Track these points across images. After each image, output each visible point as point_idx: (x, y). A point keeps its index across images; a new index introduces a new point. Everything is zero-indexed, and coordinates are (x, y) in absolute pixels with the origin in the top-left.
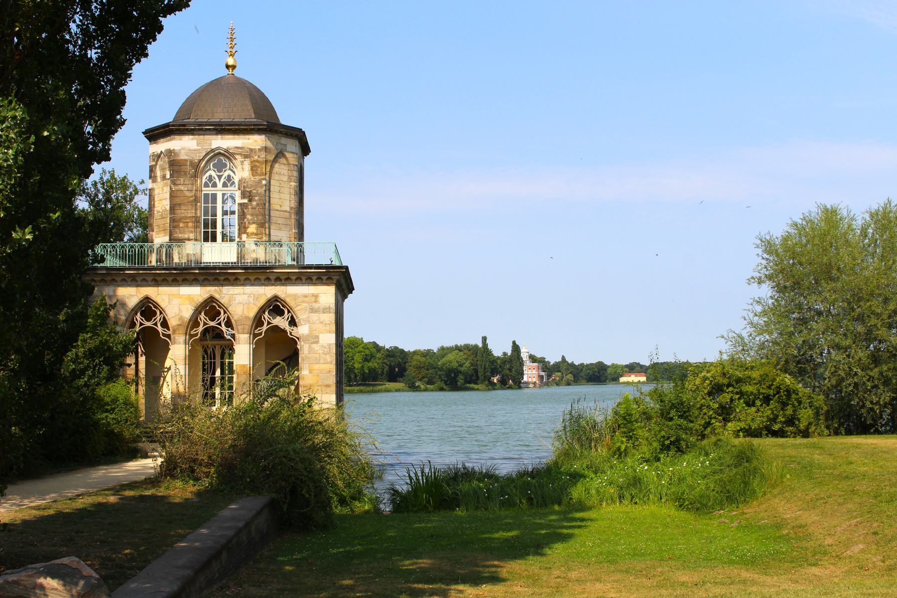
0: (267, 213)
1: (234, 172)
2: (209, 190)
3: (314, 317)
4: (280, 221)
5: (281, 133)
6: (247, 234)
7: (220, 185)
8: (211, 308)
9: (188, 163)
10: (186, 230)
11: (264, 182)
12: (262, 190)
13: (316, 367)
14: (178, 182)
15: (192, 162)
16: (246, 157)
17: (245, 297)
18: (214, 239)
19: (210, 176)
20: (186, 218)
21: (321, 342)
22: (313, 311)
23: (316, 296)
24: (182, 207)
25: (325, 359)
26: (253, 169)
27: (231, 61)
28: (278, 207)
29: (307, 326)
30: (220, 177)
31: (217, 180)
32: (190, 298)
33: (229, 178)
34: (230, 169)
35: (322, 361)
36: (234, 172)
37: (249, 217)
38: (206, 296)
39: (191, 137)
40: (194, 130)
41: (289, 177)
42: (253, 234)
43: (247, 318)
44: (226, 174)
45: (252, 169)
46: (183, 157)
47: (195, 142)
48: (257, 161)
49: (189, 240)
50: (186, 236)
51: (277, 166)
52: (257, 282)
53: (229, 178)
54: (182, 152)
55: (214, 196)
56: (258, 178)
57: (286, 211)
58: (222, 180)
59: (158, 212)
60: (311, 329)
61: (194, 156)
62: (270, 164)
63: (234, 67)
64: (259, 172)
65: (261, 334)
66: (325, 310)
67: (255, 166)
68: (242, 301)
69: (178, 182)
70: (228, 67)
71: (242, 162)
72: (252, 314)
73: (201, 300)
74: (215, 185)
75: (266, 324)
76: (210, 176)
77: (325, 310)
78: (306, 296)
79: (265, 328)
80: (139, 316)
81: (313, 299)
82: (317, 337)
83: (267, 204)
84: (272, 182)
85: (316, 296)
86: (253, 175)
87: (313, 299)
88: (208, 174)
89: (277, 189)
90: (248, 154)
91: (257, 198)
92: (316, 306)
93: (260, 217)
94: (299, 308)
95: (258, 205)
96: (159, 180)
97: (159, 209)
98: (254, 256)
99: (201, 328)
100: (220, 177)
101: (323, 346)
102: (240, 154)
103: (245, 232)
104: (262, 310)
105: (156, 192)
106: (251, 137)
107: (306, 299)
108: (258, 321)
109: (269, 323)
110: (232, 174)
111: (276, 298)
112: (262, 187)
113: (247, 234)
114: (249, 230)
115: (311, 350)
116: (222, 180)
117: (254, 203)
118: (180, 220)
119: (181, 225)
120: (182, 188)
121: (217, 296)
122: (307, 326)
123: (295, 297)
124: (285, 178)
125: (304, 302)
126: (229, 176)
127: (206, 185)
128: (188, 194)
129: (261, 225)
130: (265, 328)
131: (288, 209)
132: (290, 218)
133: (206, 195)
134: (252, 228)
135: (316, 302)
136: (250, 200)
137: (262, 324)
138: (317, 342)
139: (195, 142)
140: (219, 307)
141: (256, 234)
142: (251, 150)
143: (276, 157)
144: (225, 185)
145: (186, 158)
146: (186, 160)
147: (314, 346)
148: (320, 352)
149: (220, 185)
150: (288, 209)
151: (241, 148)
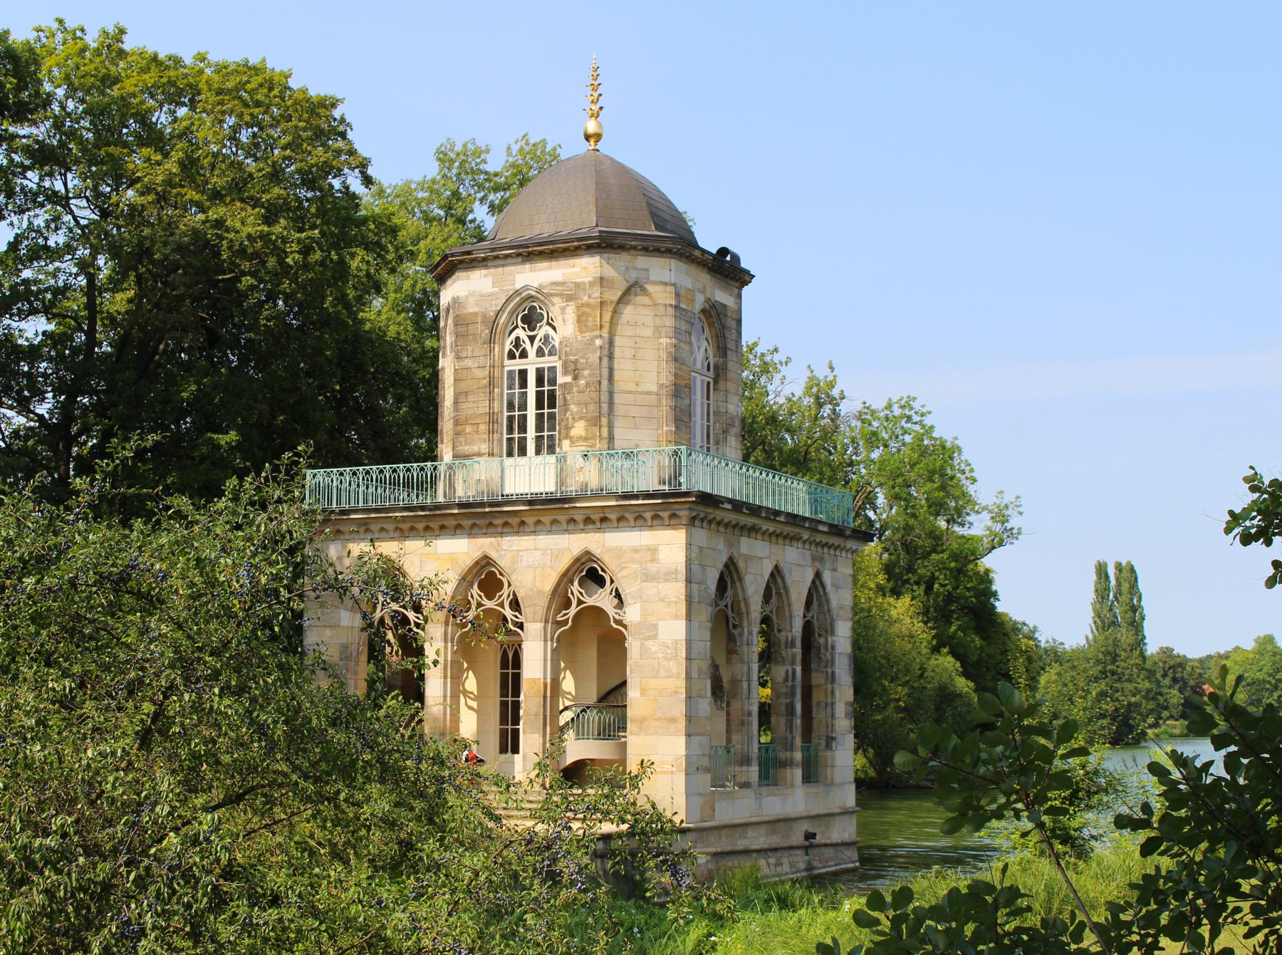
0: (605, 397)
1: (554, 328)
3: (650, 589)
4: (635, 411)
5: (634, 248)
6: (571, 439)
8: (487, 577)
10: (476, 437)
11: (598, 342)
12: (594, 358)
13: (653, 683)
14: (464, 355)
15: (484, 316)
16: (569, 298)
17: (538, 554)
18: (523, 452)
19: (518, 339)
20: (476, 416)
21: (660, 636)
22: (648, 577)
23: (653, 550)
24: (471, 398)
26: (581, 320)
27: (592, 127)
28: (632, 387)
29: (638, 606)
30: (532, 339)
31: (527, 345)
32: (452, 558)
33: (546, 339)
34: (548, 324)
36: (554, 328)
37: (573, 408)
38: (476, 555)
39: (484, 272)
40: (485, 259)
41: (657, 329)
42: (580, 438)
43: (540, 592)
45: (579, 321)
46: (471, 308)
47: (490, 280)
48: (587, 305)
49: (479, 455)
50: (475, 449)
51: (628, 312)
52: (554, 527)
53: (546, 339)
54: (471, 300)
55: (523, 374)
56: (588, 335)
57: (649, 393)
58: (537, 343)
60: (644, 613)
62: (610, 308)
63: (598, 137)
64: (590, 324)
65: (566, 621)
66: (669, 576)
67: (584, 314)
68: (532, 562)
69: (464, 355)
70: (587, 137)
71: (563, 309)
72: (548, 586)
73: (469, 562)
74: (524, 355)
76: (518, 339)
77: (669, 576)
78: (636, 551)
79: (573, 610)
81: (648, 556)
82: (655, 627)
83: (605, 383)
84: (618, 341)
85: (653, 550)
86: (581, 331)
87: (648, 556)
89: (629, 353)
90: (570, 293)
91: (586, 373)
92: (653, 568)
93: (592, 407)
94: (625, 572)
95: (587, 384)
98: (580, 478)
100: (532, 339)
102: (561, 295)
103: (567, 437)
104: (566, 578)
107: (637, 556)
108: (560, 598)
109: (580, 602)
112: (594, 352)
113: (571, 439)
114: (574, 432)
115: (644, 652)
117: (582, 382)
118: (466, 422)
119: (468, 429)
122: (638, 606)
123: (619, 552)
124: (648, 332)
125: (633, 561)
126: (546, 337)
127: (511, 356)
129: (595, 422)
130: (573, 610)
131: (654, 389)
132: (659, 404)
135: (652, 561)
136: (575, 378)
137: (567, 604)
138: (655, 637)
139: (490, 280)
140: (603, 570)
141: (585, 439)
142: (577, 285)
143: (627, 292)
144: (540, 353)
146: (476, 314)
147: (650, 643)
148: (660, 655)
149: (532, 352)
150: (654, 389)
151: (562, 284)
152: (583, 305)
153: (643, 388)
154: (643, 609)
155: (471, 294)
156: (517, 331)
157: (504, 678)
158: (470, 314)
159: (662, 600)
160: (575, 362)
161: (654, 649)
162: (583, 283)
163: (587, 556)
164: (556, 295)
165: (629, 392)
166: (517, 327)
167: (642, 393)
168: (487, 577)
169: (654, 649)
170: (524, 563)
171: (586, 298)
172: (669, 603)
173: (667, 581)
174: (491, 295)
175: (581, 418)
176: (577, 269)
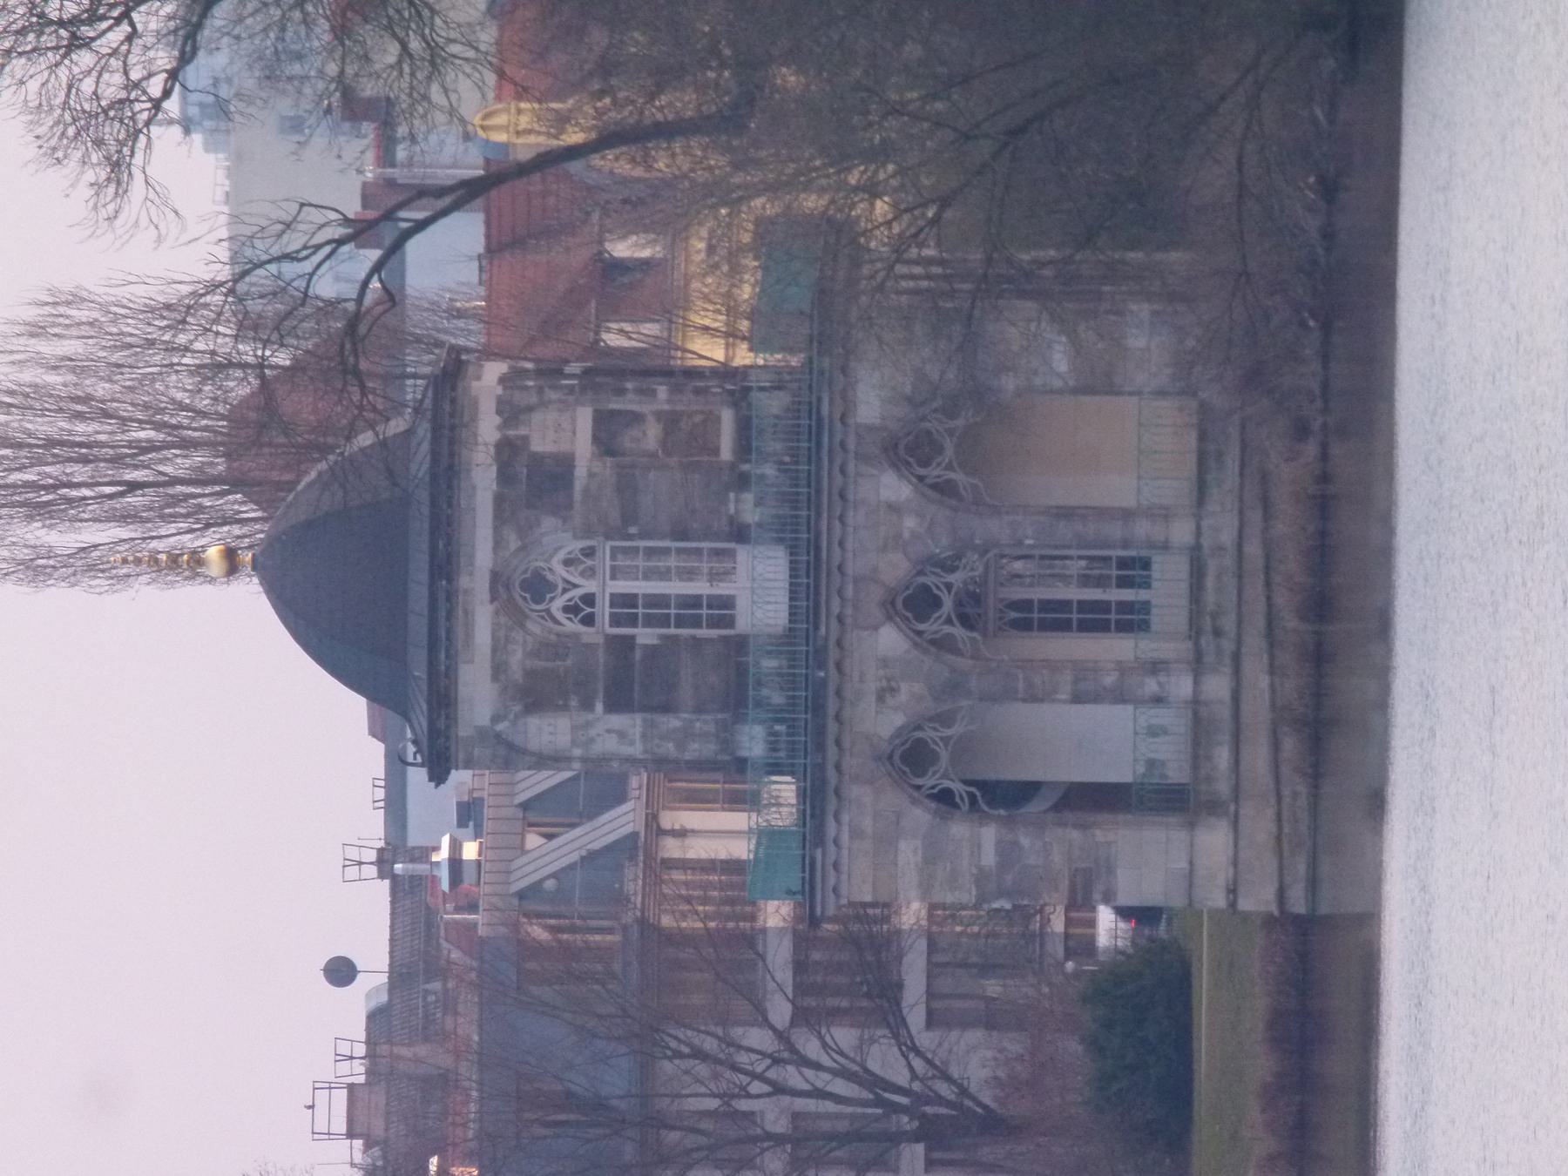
2: (604, 611)
19: (566, 609)
34: (548, 561)
36: (557, 549)
44: (560, 570)
74: (589, 599)
76: (566, 609)
79: (958, 477)
80: (927, 781)
88: (560, 616)
99: (958, 631)
110: (562, 555)
127: (589, 620)
133: (616, 621)
144: (590, 573)
149: (590, 586)
157: (1045, 626)
166: (548, 611)
168: (915, 604)
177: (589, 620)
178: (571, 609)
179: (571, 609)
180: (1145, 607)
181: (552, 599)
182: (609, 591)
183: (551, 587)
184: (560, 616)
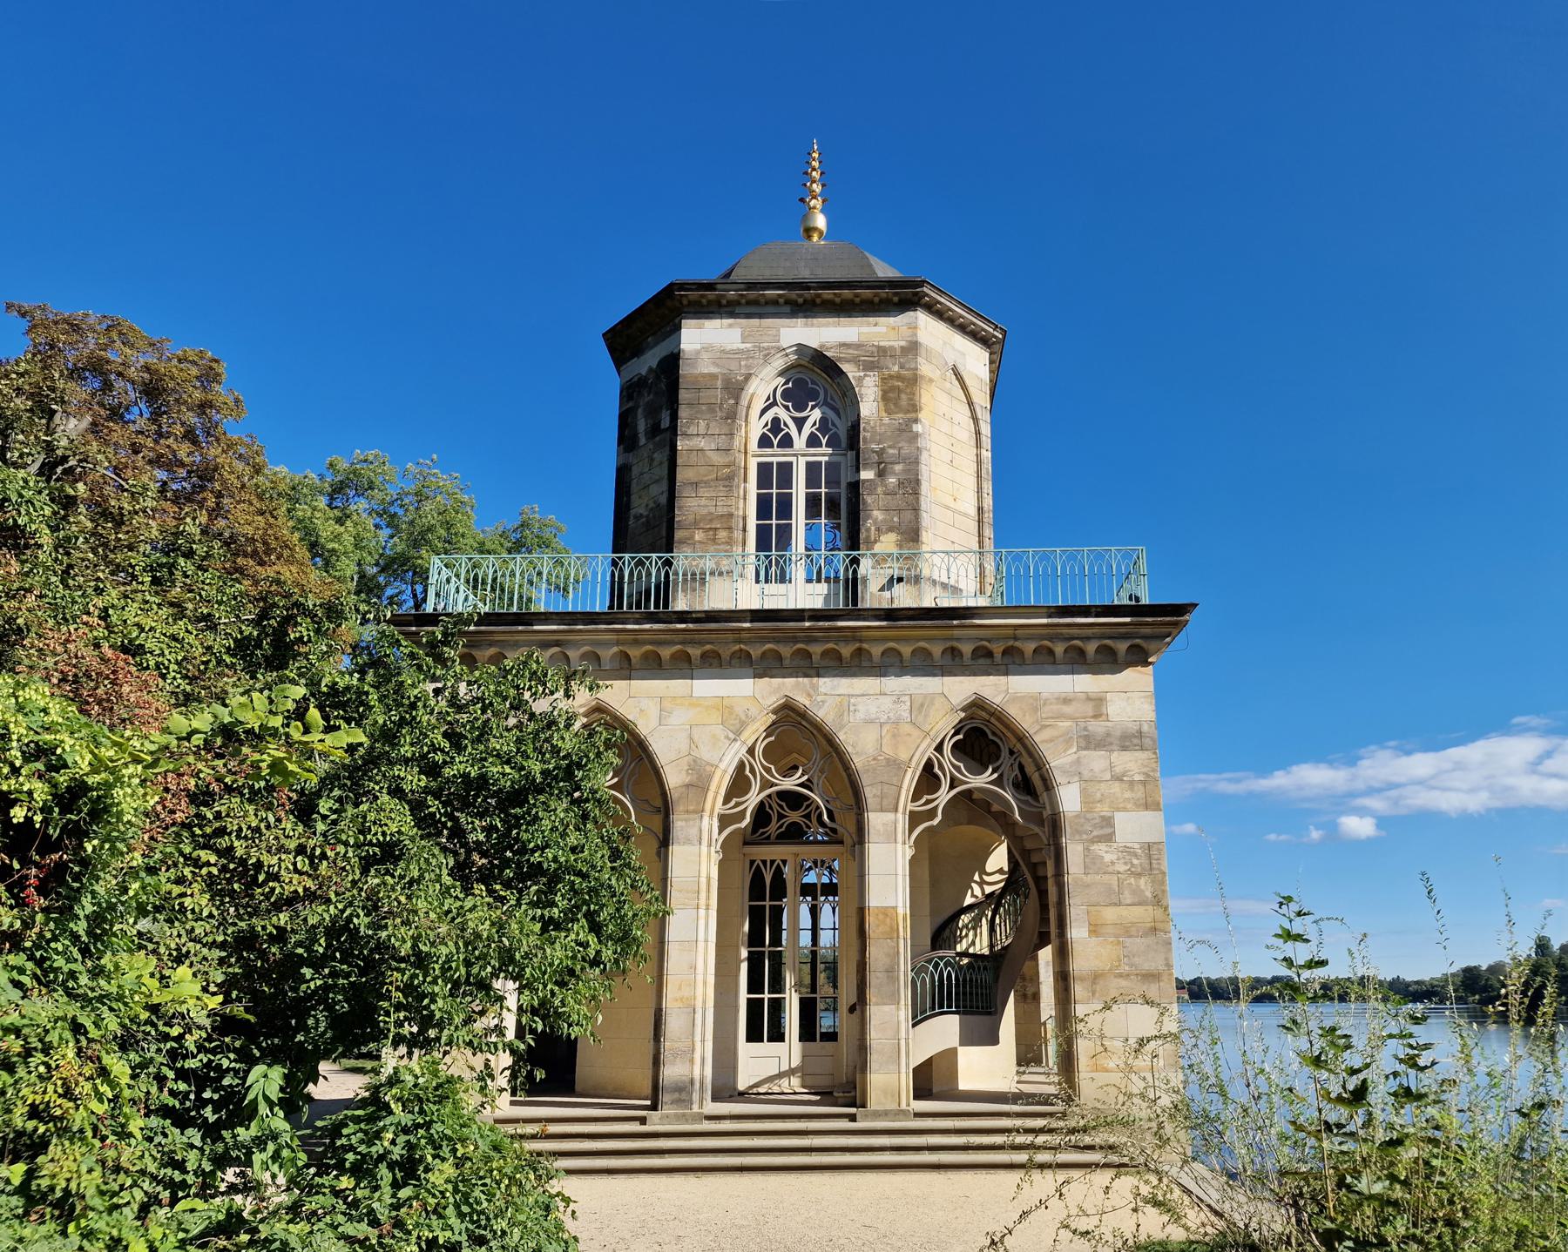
2: (775, 456)
3: (1096, 761)
7: (800, 442)
9: (719, 384)
13: (1110, 914)
16: (869, 367)
17: (887, 702)
19: (776, 421)
22: (1090, 742)
24: (703, 492)
25: (1136, 891)
30: (800, 423)
35: (1127, 897)
38: (774, 701)
39: (727, 322)
40: (731, 303)
48: (899, 377)
54: (705, 355)
55: (786, 470)
58: (807, 429)
59: (638, 517)
61: (734, 366)
67: (893, 389)
74: (787, 442)
75: (945, 785)
76: (776, 421)
78: (1066, 701)
79: (944, 796)
82: (1108, 822)
87: (1089, 709)
88: (769, 415)
91: (898, 468)
92: (1097, 727)
95: (900, 484)
96: (643, 441)
97: (642, 511)
100: (800, 423)
101: (1127, 851)
105: (635, 471)
106: (882, 320)
107: (1067, 709)
111: (977, 706)
114: (878, 548)
115: (1091, 862)
116: (807, 429)
120: (702, 443)
121: (802, 700)
123: (1036, 703)
125: (1061, 716)
128: (717, 458)
130: (944, 796)
134: (887, 544)
135: (1096, 716)
138: (1109, 838)
142: (882, 351)
145: (714, 370)
146: (713, 376)
147: (1100, 849)
148: (1122, 868)
149: (800, 442)
151: (858, 346)
152: (891, 377)
153: (960, 506)
154: (1083, 791)
155: (705, 349)
156: (775, 409)
158: (704, 375)
159: (1118, 778)
160: (881, 453)
161: (1108, 858)
162: (892, 348)
163: (977, 706)
164: (848, 361)
165: (948, 508)
166: (774, 403)
167: (960, 513)
169: (1108, 858)
170: (861, 715)
171: (896, 368)
172: (1132, 783)
173: (1124, 748)
174: (739, 352)
175: (890, 530)
176: (881, 329)
177: (764, 442)
178: (776, 425)
179: (776, 425)
180: (777, 1036)
181: (787, 408)
182: (793, 459)
183: (800, 407)
184: (769, 415)
